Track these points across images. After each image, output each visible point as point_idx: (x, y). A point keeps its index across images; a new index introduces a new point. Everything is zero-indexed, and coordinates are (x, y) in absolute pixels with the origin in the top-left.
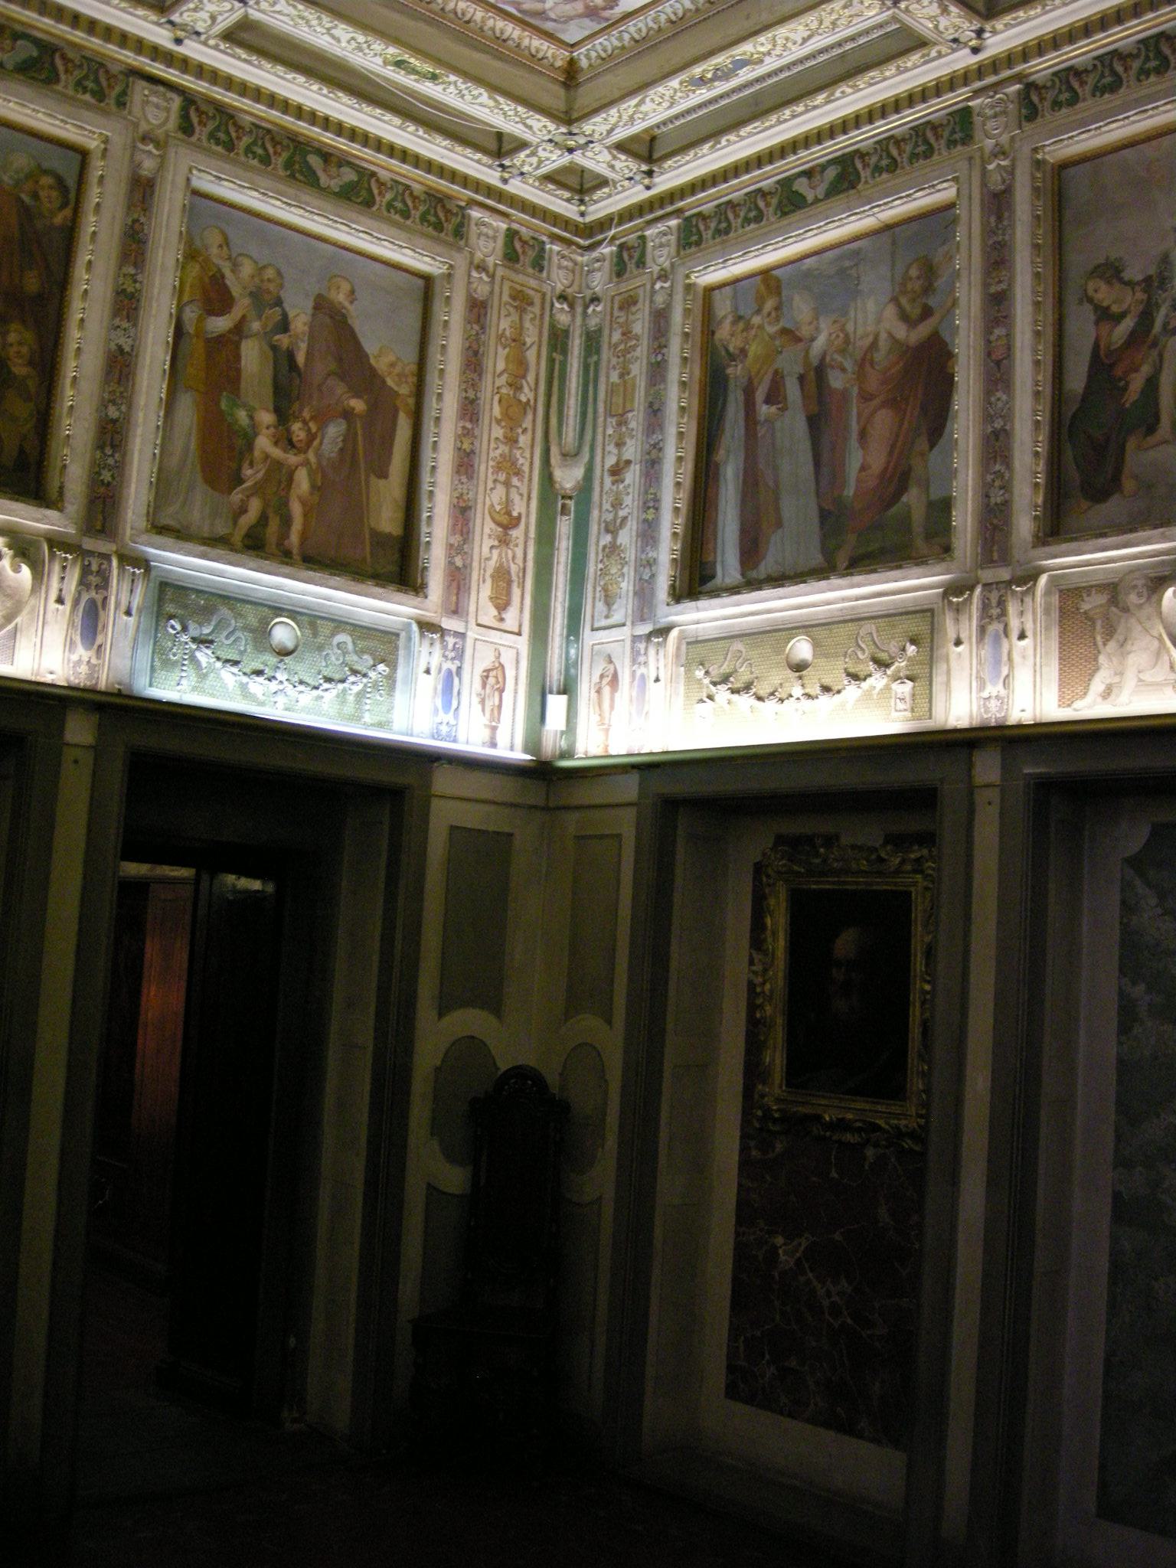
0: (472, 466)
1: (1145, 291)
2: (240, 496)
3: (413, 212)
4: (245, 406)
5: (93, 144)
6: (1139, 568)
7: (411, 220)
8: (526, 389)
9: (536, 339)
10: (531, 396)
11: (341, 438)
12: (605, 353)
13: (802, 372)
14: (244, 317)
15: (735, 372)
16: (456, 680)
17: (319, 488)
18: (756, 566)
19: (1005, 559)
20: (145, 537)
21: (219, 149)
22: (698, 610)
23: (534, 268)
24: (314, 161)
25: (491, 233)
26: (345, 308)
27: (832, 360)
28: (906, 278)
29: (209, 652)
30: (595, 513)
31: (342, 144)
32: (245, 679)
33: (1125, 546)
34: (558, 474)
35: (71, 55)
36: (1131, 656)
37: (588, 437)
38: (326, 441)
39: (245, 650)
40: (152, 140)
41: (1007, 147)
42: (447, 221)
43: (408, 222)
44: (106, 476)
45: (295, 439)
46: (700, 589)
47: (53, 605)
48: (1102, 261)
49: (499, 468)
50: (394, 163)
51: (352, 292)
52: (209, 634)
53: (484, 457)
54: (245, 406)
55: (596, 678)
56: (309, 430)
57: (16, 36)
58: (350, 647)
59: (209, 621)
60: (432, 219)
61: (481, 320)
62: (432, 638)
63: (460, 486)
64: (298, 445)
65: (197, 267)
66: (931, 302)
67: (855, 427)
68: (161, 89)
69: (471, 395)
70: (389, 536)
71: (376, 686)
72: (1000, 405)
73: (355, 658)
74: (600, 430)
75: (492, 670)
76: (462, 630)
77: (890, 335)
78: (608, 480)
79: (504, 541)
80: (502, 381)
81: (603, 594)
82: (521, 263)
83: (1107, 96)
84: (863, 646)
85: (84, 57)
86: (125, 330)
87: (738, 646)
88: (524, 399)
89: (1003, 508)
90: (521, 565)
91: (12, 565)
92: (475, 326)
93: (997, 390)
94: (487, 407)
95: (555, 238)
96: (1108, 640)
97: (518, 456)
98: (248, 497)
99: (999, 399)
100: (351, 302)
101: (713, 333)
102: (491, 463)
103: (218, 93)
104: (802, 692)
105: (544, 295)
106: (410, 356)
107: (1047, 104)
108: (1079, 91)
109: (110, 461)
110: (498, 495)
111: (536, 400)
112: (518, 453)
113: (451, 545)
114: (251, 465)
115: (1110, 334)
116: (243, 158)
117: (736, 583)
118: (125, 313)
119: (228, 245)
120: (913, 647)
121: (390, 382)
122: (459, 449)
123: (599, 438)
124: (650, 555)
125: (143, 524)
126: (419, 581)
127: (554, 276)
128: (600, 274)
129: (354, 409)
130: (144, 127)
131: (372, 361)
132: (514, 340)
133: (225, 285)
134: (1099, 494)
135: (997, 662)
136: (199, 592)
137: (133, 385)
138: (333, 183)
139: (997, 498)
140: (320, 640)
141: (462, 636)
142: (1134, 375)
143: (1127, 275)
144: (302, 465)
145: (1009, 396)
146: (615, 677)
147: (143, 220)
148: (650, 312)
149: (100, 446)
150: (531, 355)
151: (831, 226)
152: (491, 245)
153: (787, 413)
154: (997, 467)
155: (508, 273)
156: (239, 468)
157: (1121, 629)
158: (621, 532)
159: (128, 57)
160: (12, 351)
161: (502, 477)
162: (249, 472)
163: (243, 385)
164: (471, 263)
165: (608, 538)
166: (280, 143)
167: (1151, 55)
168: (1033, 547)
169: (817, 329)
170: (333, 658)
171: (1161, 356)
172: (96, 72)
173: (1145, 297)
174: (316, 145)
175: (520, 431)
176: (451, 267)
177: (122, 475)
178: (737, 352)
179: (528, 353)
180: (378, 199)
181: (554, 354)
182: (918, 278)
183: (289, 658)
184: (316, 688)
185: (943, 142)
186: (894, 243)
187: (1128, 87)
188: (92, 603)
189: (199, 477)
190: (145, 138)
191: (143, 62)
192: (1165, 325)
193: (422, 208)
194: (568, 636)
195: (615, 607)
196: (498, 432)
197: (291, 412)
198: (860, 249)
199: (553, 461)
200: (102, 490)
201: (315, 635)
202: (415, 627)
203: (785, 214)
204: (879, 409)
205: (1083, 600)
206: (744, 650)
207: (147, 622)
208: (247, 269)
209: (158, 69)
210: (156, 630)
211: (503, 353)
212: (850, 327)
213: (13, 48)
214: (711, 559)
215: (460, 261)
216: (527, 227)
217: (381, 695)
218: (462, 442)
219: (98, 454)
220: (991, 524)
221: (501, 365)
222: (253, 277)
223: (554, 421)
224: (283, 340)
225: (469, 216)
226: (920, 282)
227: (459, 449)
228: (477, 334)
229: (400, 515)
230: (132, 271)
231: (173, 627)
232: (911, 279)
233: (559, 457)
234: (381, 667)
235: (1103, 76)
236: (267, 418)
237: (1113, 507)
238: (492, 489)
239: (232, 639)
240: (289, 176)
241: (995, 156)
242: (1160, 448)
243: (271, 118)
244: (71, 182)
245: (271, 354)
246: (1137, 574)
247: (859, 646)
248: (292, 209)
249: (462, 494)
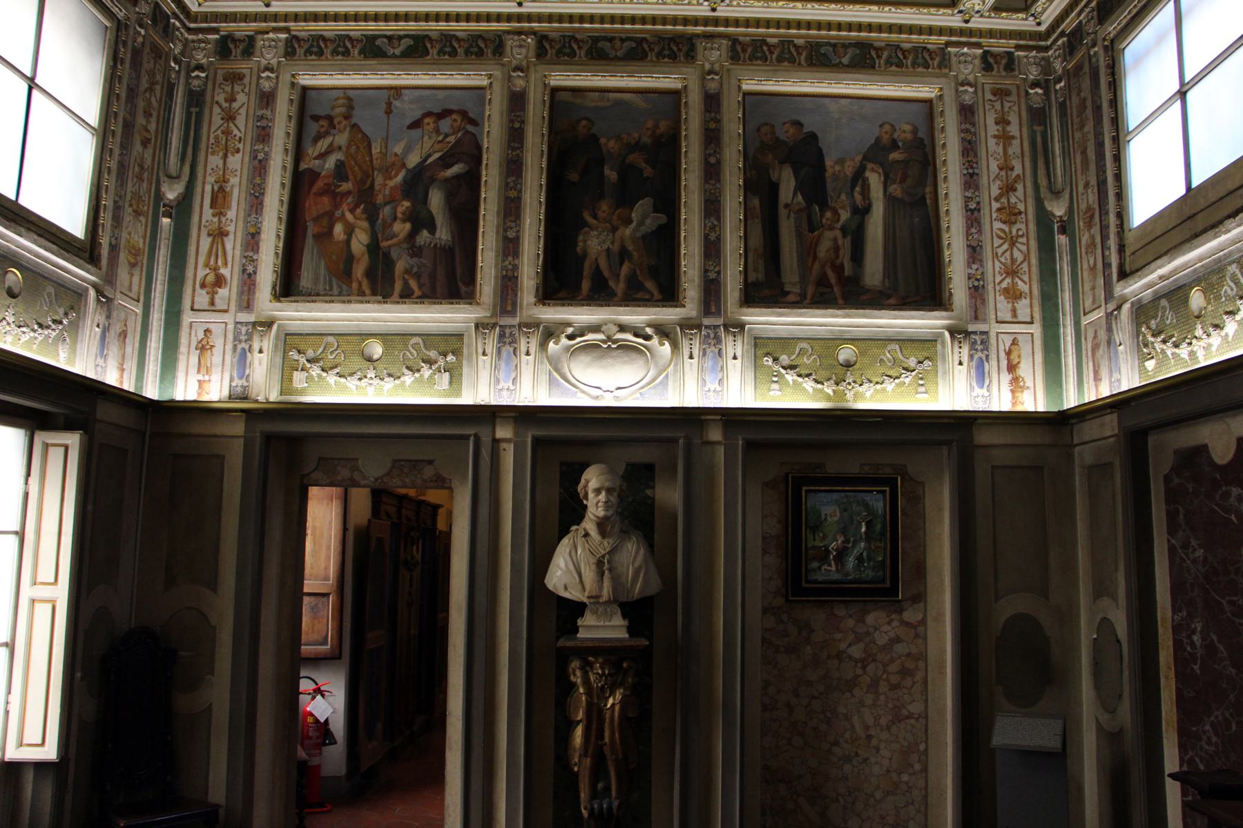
5: (679, 85)
16: (986, 364)
130: (707, 66)
190: (710, 72)
202: (947, 334)
248: (816, 84)
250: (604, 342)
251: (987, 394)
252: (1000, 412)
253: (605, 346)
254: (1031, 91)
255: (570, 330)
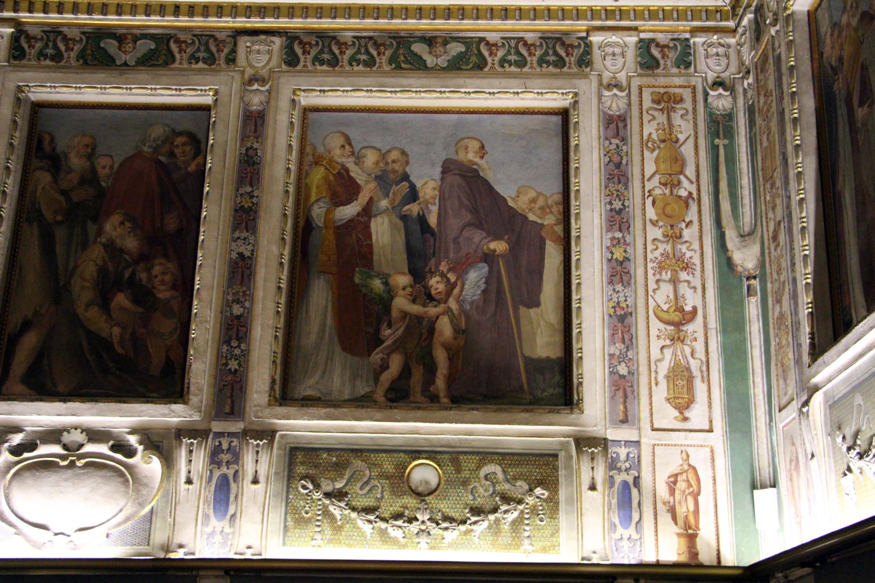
0: (628, 273)
2: (381, 355)
3: (529, 59)
4: (379, 275)
5: (208, 100)
7: (529, 65)
8: (685, 183)
9: (692, 133)
10: (693, 189)
11: (484, 280)
14: (371, 199)
16: (635, 492)
17: (464, 331)
20: (267, 411)
21: (325, 67)
23: (679, 67)
24: (418, 48)
25: (617, 50)
26: (476, 164)
29: (343, 504)
31: (440, 24)
32: (383, 525)
34: (737, 257)
35: (182, 37)
38: (466, 287)
39: (382, 497)
40: (257, 80)
42: (568, 55)
43: (526, 69)
44: (233, 365)
45: (433, 292)
47: (183, 487)
49: (661, 268)
50: (497, 23)
51: (482, 147)
52: (344, 487)
53: (640, 260)
54: (379, 275)
56: (448, 280)
57: (136, 39)
58: (500, 476)
59: (341, 476)
60: (552, 58)
61: (621, 133)
62: (593, 452)
63: (615, 296)
64: (437, 297)
65: (322, 169)
68: (263, 37)
69: (617, 205)
70: (548, 359)
71: (534, 511)
73: (507, 486)
75: (681, 474)
76: (636, 439)
79: (678, 339)
80: (656, 181)
82: (662, 67)
85: (194, 35)
86: (245, 239)
88: (683, 193)
90: (704, 359)
91: (143, 457)
92: (613, 141)
94: (638, 212)
95: (695, 31)
97: (684, 250)
98: (388, 355)
100: (482, 157)
102: (650, 265)
103: (313, 23)
105: (694, 88)
106: (553, 189)
109: (237, 352)
110: (663, 296)
111: (699, 190)
112: (684, 248)
113: (611, 356)
114: (390, 326)
116: (348, 68)
118: (244, 225)
119: (350, 144)
121: (532, 217)
122: (610, 260)
125: (264, 399)
126: (576, 397)
127: (701, 64)
129: (495, 251)
130: (249, 72)
131: (511, 203)
132: (664, 141)
133: (350, 178)
136: (329, 450)
137: (254, 284)
138: (439, 61)
140: (465, 474)
141: (638, 443)
144: (443, 314)
147: (255, 146)
149: (228, 342)
150: (687, 150)
152: (620, 61)
155: (645, 81)
156: (378, 331)
159: (228, 22)
160: (157, 281)
161: (667, 275)
162: (388, 332)
163: (375, 258)
164: (600, 84)
166: (383, 45)
170: (481, 490)
172: (207, 44)
174: (419, 34)
175: (683, 225)
176: (576, 94)
177: (247, 361)
179: (682, 148)
180: (489, 60)
181: (717, 141)
183: (431, 497)
184: (464, 522)
188: (224, 479)
189: (338, 348)
190: (252, 80)
191: (241, 22)
193: (538, 53)
196: (655, 233)
197: (427, 269)
199: (730, 245)
200: (230, 378)
201: (459, 471)
207: (282, 486)
208: (371, 158)
209: (255, 23)
210: (288, 492)
211: (650, 158)
213: (134, 48)
215: (587, 87)
216: (661, 32)
217: (541, 520)
218: (612, 253)
219: (225, 348)
221: (650, 169)
222: (377, 163)
223: (726, 206)
224: (414, 209)
225: (591, 42)
227: (610, 260)
228: (618, 147)
229: (559, 339)
230: (249, 189)
231: (305, 487)
233: (737, 240)
234: (538, 491)
236: (402, 280)
238: (654, 291)
239: (368, 488)
240: (396, 68)
243: (369, 27)
244: (201, 136)
245: (400, 223)
249: (618, 303)
250: (63, 457)
251: (635, 536)
252: (658, 565)
253: (65, 463)
254: (712, 93)
255: (17, 439)
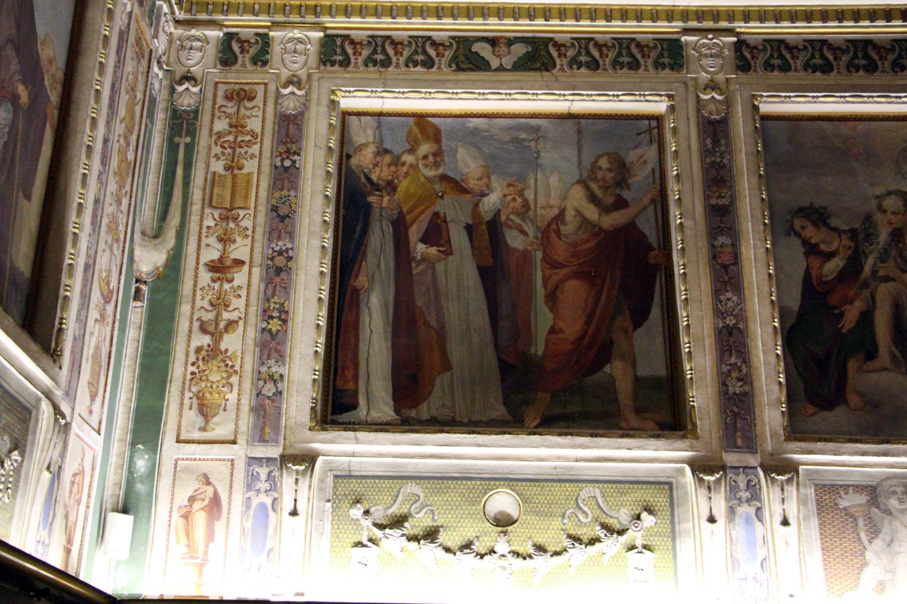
1: (851, 239)
6: (895, 476)
12: (204, 140)
13: (471, 222)
15: (380, 202)
18: (415, 405)
19: (751, 446)
22: (357, 441)
27: (508, 218)
28: (594, 167)
30: (185, 309)
33: (885, 454)
36: (901, 556)
37: (174, 220)
41: (723, 86)
46: (334, 417)
48: (806, 205)
55: (182, 498)
66: (625, 194)
67: (540, 292)
72: (730, 304)
74: (194, 220)
77: (579, 213)
78: (205, 277)
81: (195, 401)
83: (818, 73)
84: (585, 509)
87: (412, 488)
89: (743, 398)
93: (727, 291)
96: (873, 538)
99: (729, 299)
101: (349, 157)
104: (509, 549)
107: (887, 64)
108: (792, 62)
115: (821, 267)
117: (388, 419)
120: (652, 517)
123: (194, 226)
124: (274, 369)
128: (199, 55)
134: (828, 404)
135: (752, 544)
139: (736, 387)
142: (848, 307)
143: (834, 222)
145: (740, 298)
146: (216, 501)
148: (275, 114)
151: (360, 94)
153: (450, 257)
154: (733, 360)
157: (885, 529)
158: (226, 337)
165: (206, 340)
167: (860, 55)
168: (786, 440)
169: (488, 186)
171: (873, 297)
173: (852, 244)
178: (382, 183)
182: (609, 170)
185: (650, 62)
186: (579, 132)
187: (838, 72)
192: (874, 272)
194: (133, 444)
195: (216, 419)
198: (538, 129)
203: (460, 69)
204: (569, 278)
205: (840, 497)
206: (422, 495)
212: (529, 195)
214: (350, 385)
220: (731, 411)
226: (613, 174)
232: (600, 168)
235: (813, 57)
237: (837, 416)
241: (713, 89)
242: (883, 373)
246: (895, 482)
247: (580, 508)
